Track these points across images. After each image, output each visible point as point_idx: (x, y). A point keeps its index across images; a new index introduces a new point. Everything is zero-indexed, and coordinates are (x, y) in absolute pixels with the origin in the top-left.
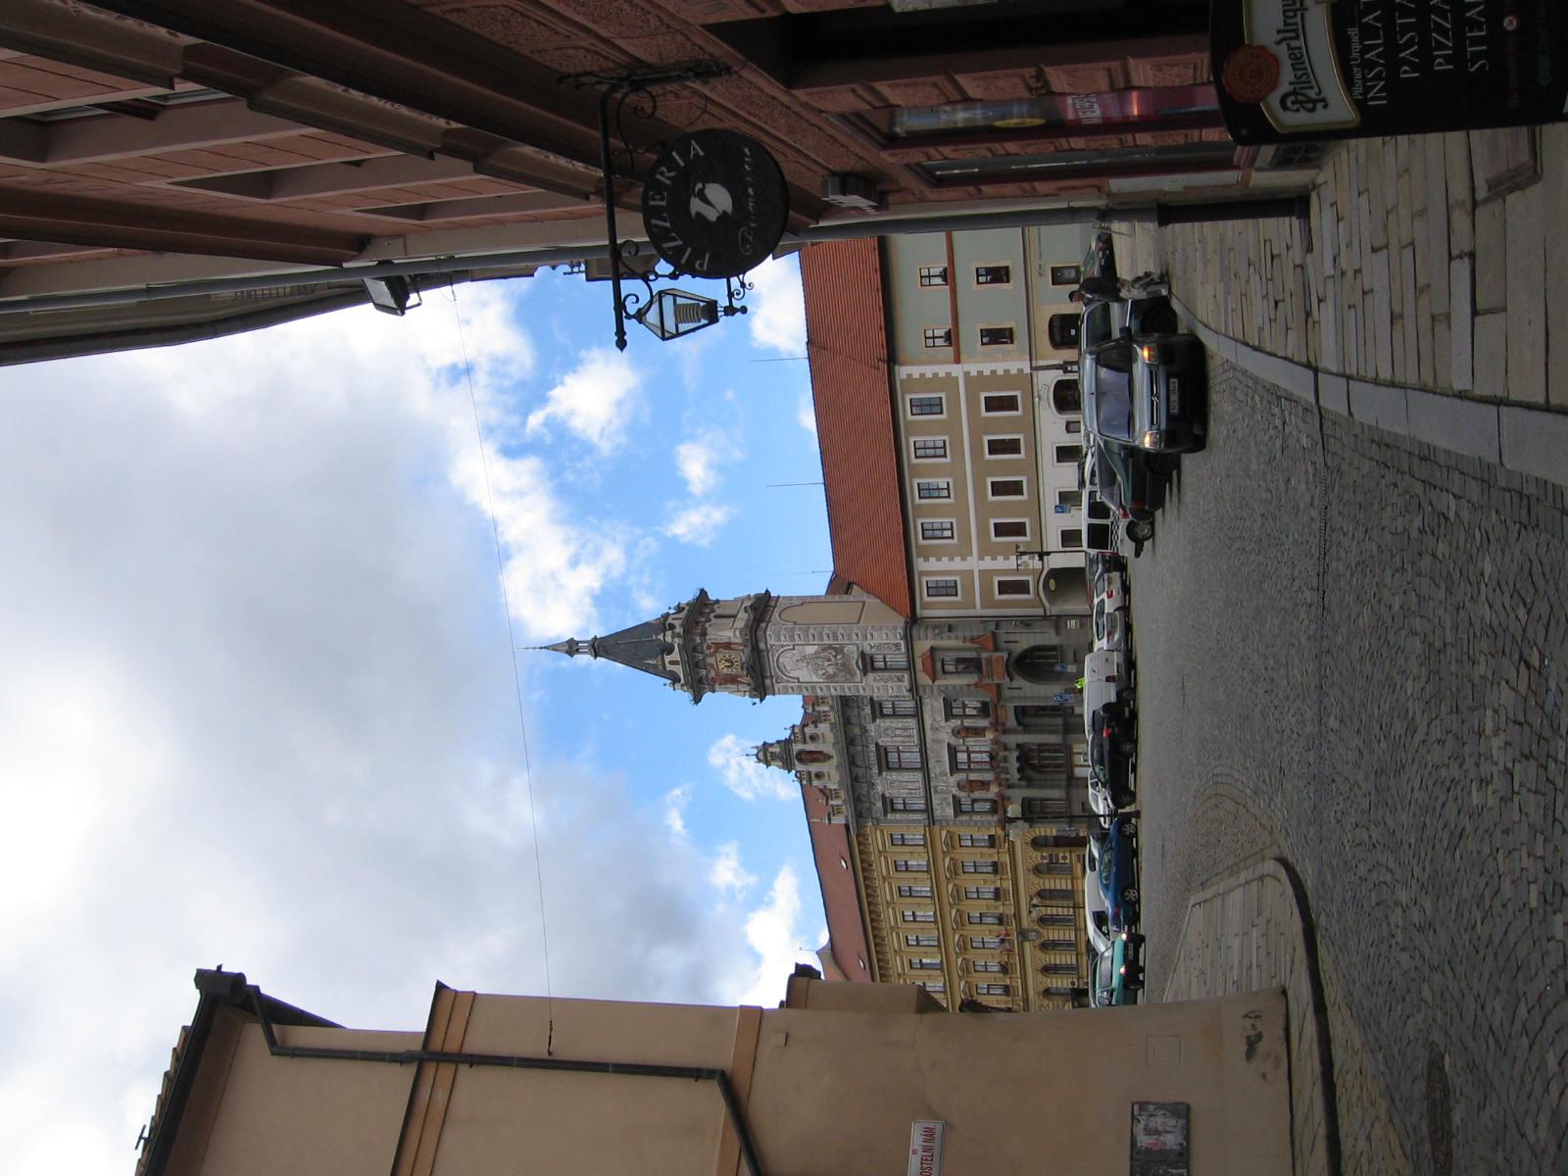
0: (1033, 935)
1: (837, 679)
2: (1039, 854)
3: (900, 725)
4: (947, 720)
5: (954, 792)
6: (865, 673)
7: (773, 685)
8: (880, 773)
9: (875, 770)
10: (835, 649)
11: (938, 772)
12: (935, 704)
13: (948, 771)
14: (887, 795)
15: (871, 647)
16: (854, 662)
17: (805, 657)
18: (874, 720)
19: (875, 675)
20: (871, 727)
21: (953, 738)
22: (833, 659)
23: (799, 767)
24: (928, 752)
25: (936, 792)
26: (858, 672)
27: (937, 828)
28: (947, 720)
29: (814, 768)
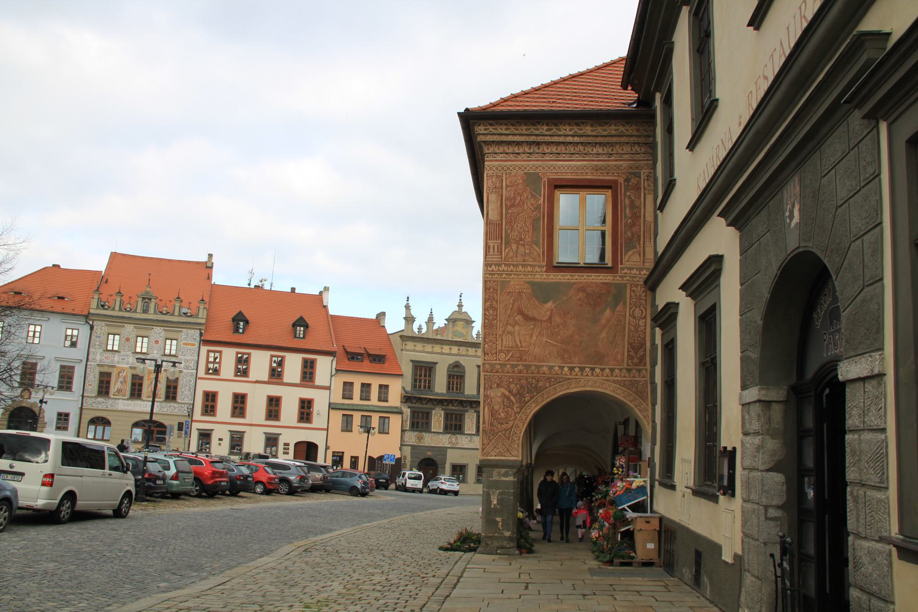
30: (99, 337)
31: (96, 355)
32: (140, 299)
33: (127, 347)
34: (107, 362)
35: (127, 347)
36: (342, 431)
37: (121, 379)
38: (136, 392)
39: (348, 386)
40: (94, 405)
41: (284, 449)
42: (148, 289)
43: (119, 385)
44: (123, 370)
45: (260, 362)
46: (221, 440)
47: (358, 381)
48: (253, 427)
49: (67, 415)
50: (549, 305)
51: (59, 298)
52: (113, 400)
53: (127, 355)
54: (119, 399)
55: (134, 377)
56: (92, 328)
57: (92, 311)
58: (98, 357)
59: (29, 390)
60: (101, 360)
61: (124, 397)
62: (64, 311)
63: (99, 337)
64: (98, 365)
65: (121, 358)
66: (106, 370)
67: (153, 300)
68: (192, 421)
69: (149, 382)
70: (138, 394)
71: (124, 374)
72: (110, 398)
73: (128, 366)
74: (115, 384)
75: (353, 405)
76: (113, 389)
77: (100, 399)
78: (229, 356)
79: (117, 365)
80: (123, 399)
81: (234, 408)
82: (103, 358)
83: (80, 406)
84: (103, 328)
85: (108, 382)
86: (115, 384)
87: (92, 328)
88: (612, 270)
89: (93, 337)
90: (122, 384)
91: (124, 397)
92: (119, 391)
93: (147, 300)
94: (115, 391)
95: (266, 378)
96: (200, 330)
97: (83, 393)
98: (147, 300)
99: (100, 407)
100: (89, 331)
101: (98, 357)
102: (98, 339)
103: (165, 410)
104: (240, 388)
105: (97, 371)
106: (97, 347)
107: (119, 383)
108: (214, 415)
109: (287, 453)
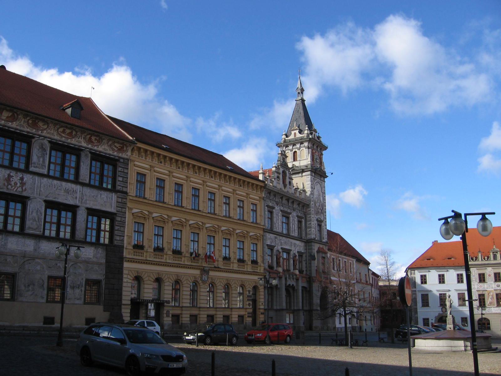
0: (205, 277)
1: (315, 207)
2: (251, 290)
3: (296, 228)
4: (298, 252)
5: (276, 247)
6: (317, 220)
7: (313, 176)
8: (281, 211)
9: (282, 208)
10: (322, 210)
11: (282, 242)
12: (302, 248)
13: (282, 247)
14: (274, 210)
15: (323, 227)
16: (319, 217)
17: (320, 195)
18: (297, 216)
19: (317, 225)
20: (294, 214)
21: (292, 253)
22: (320, 208)
23: (281, 170)
24: (288, 239)
25: (276, 238)
26: (317, 217)
27: (261, 232)
28: (298, 252)
29: (281, 176)
30: (474, 276)
31: (475, 286)
32: (492, 253)
33: (490, 279)
34: (481, 289)
35: (490, 279)
37: (490, 297)
44: (491, 291)
51: (449, 259)
52: (489, 308)
53: (491, 284)
54: (491, 307)
58: (476, 287)
59: (445, 308)
60: (478, 288)
61: (494, 306)
63: (474, 276)
64: (477, 291)
65: (488, 285)
66: (481, 293)
67: (499, 253)
79: (487, 290)
80: (494, 307)
82: (478, 287)
84: (475, 271)
85: (484, 299)
90: (492, 299)
91: (494, 306)
92: (491, 303)
93: (495, 253)
98: (495, 253)
101: (476, 287)
102: (474, 277)
106: (474, 281)
107: (490, 299)
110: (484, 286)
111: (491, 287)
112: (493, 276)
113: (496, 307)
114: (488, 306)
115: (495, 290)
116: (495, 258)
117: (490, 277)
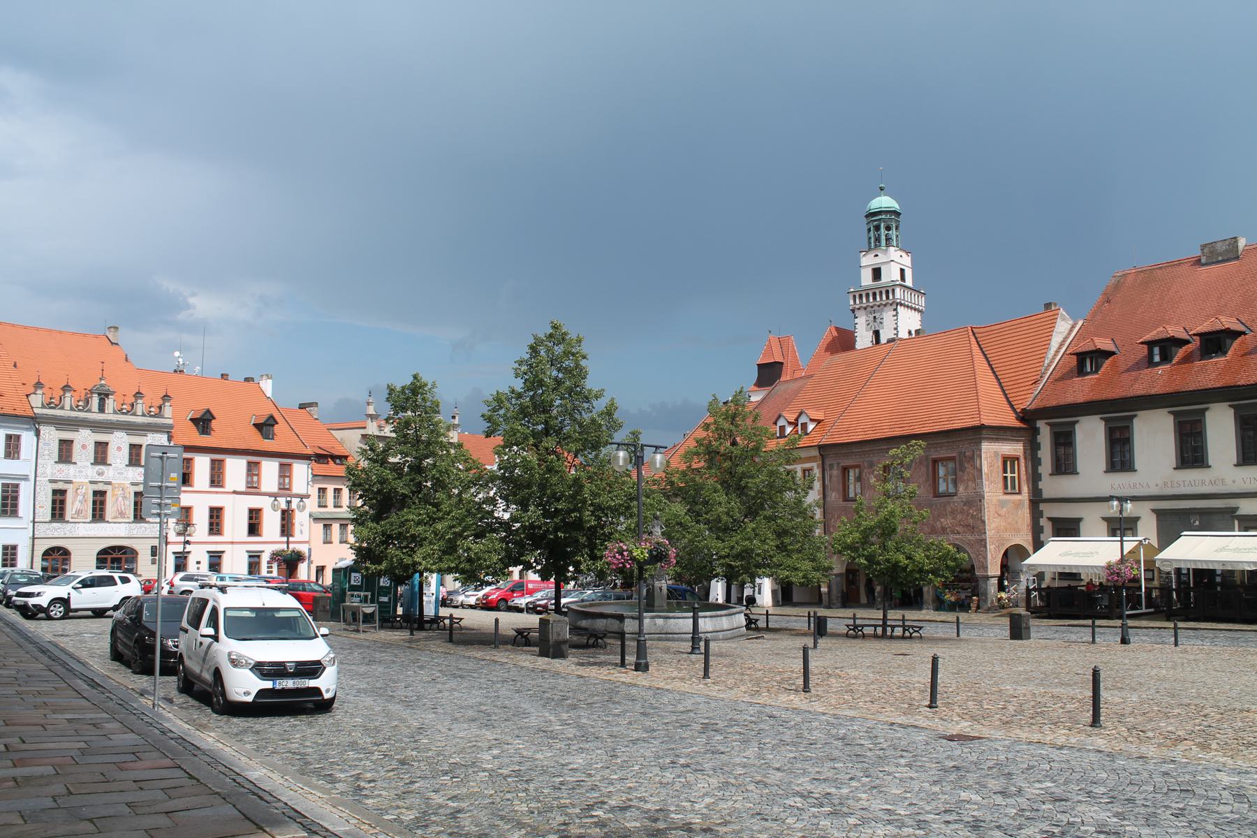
33: (83, 456)
36: (324, 543)
37: (80, 498)
38: (98, 513)
39: (322, 491)
40: (48, 532)
41: (268, 567)
42: (103, 382)
43: (78, 505)
44: (82, 484)
45: (235, 468)
46: (198, 563)
47: (330, 488)
48: (235, 546)
49: (14, 548)
50: (1004, 509)
53: (85, 467)
55: (95, 493)
56: (38, 434)
57: (36, 411)
58: (49, 471)
62: (17, 413)
63: (49, 444)
64: (52, 481)
65: (77, 470)
66: (60, 486)
68: (167, 543)
69: (114, 499)
70: (11, 511)
71: (84, 491)
72: (68, 522)
73: (87, 481)
74: (73, 504)
75: (328, 513)
76: (70, 510)
77: (55, 525)
78: (202, 465)
79: (74, 480)
81: (211, 524)
83: (31, 535)
85: (63, 502)
86: (73, 504)
87: (38, 434)
88: (1020, 493)
89: (40, 444)
92: (79, 512)
94: (74, 512)
95: (243, 488)
96: (168, 432)
97: (34, 518)
98: (103, 396)
99: (56, 534)
100: (35, 438)
101: (49, 471)
102: (47, 447)
103: (135, 532)
104: (216, 501)
105: (49, 488)
106: (47, 457)
108: (259, 535)
109: (271, 572)
110: (67, 471)
111: (84, 474)
112: (91, 448)
113: (90, 522)
114: (72, 518)
115: (91, 482)
116: (102, 409)
117: (84, 451)
